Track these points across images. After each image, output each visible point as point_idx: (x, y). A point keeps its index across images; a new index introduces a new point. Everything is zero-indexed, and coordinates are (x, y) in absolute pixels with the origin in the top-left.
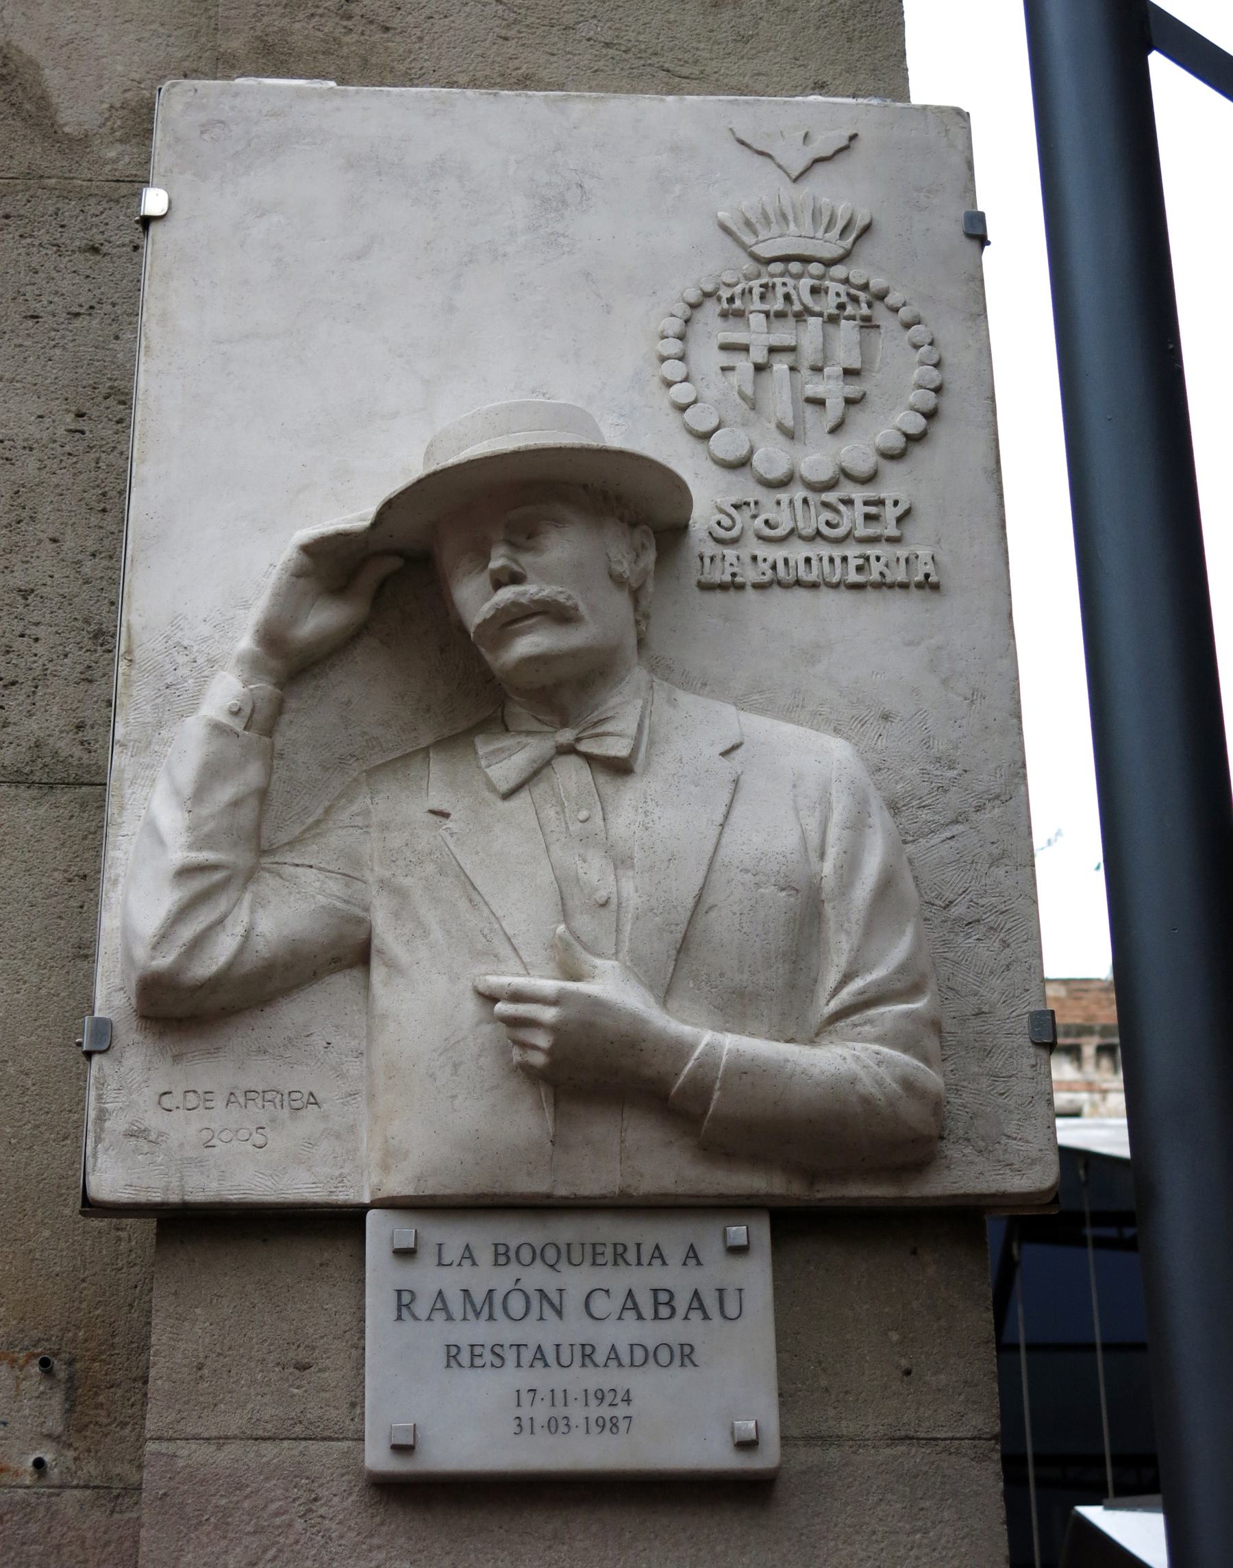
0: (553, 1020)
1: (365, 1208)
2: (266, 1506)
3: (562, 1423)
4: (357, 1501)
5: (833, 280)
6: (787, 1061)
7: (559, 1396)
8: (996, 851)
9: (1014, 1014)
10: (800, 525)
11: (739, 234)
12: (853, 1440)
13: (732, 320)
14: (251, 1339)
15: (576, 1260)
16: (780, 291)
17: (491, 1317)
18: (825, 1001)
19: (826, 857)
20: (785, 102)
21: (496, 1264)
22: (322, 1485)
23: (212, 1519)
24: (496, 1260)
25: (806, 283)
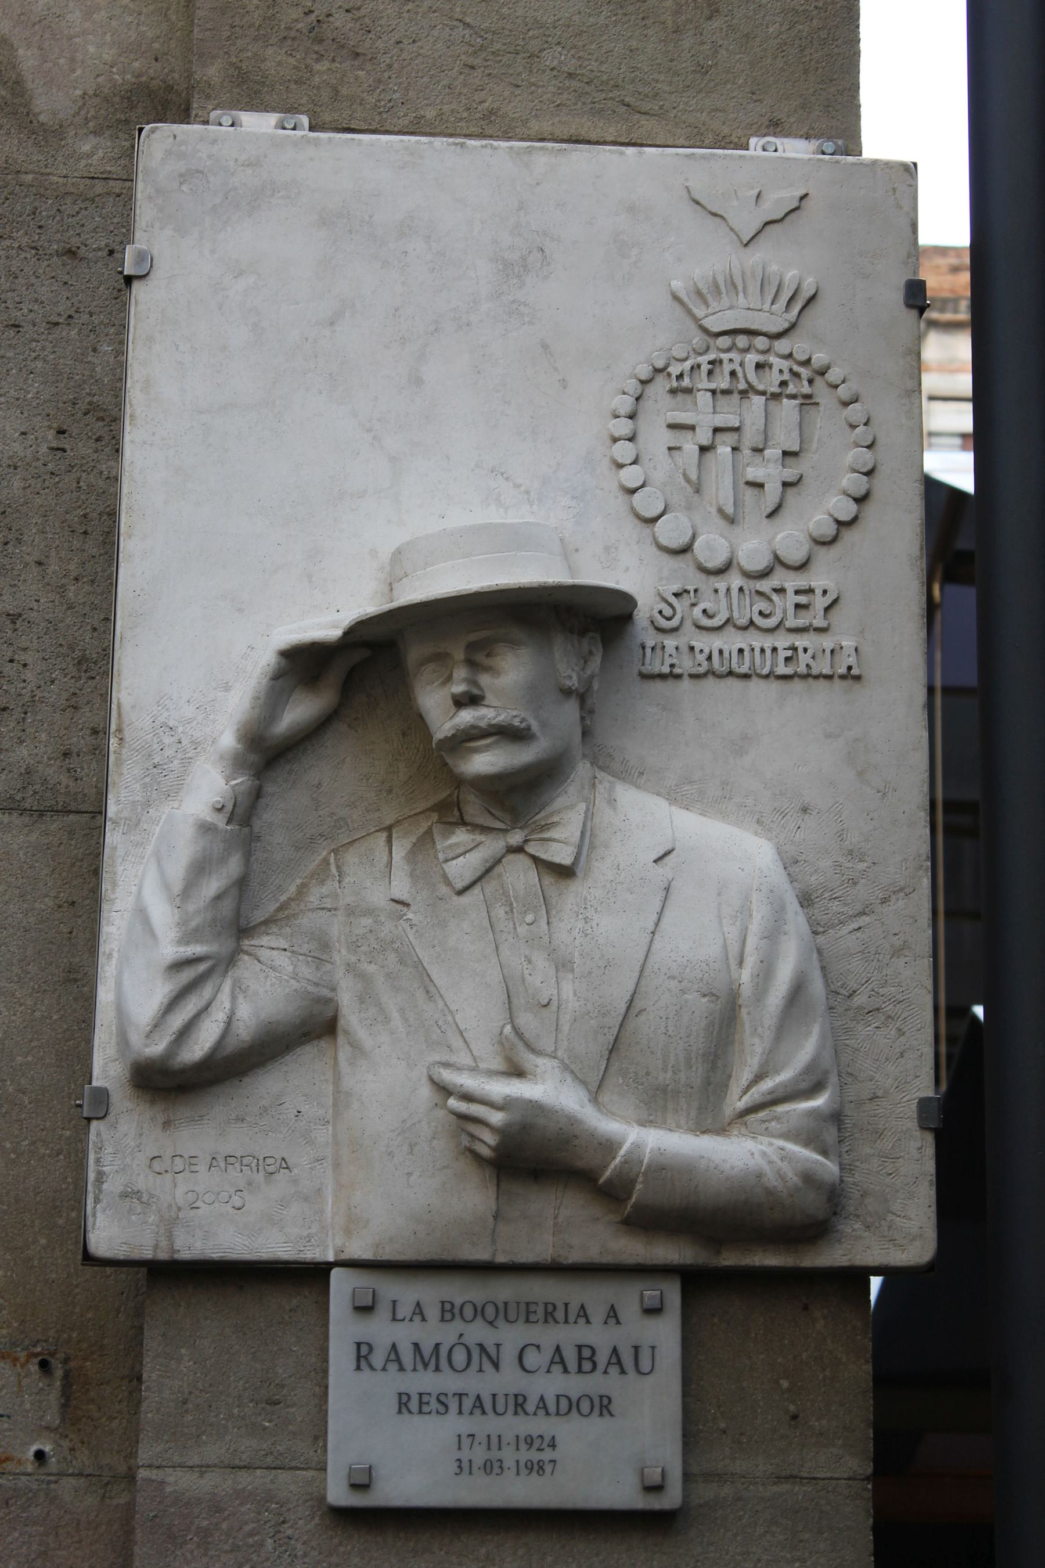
1: (330, 1266)
2: (241, 1528)
3: (496, 1465)
4: (319, 1525)
7: (494, 1440)
8: (897, 942)
9: (905, 1099)
10: (736, 615)
13: (680, 397)
16: (727, 368)
17: (437, 1369)
20: (741, 157)
21: (443, 1320)
22: (289, 1510)
23: (195, 1539)
24: (443, 1317)
25: (752, 358)
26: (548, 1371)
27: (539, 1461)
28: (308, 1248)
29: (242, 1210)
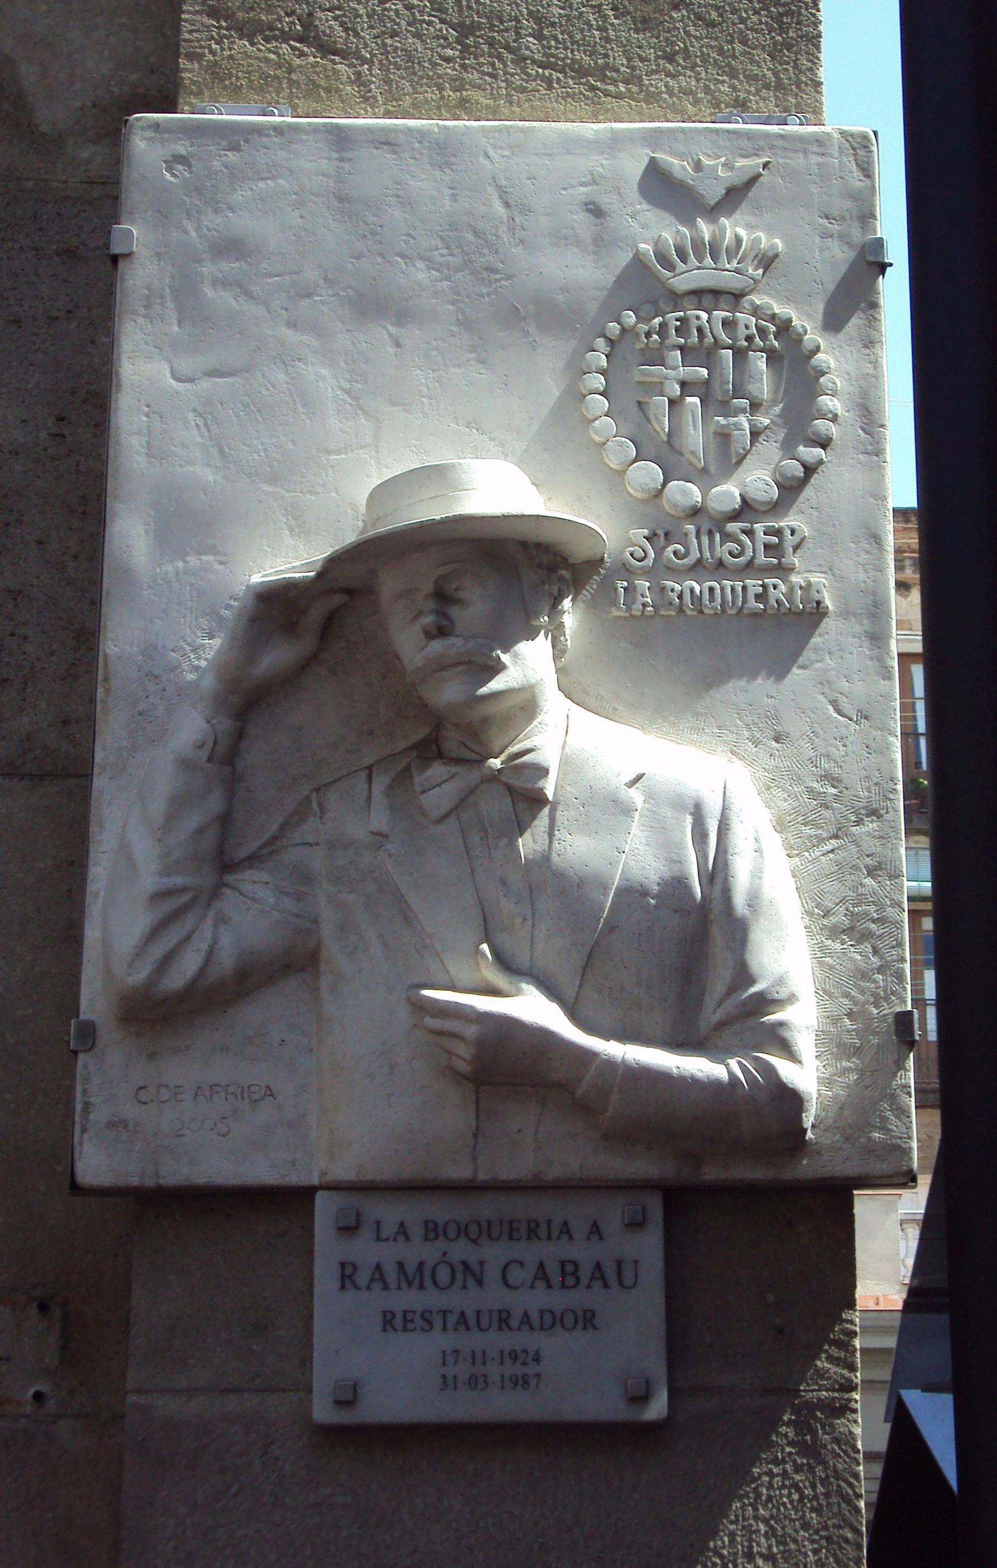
3: (481, 1380)
7: (479, 1356)
17: (421, 1286)
21: (426, 1239)
23: (183, 1461)
26: (532, 1287)
29: (227, 1137)
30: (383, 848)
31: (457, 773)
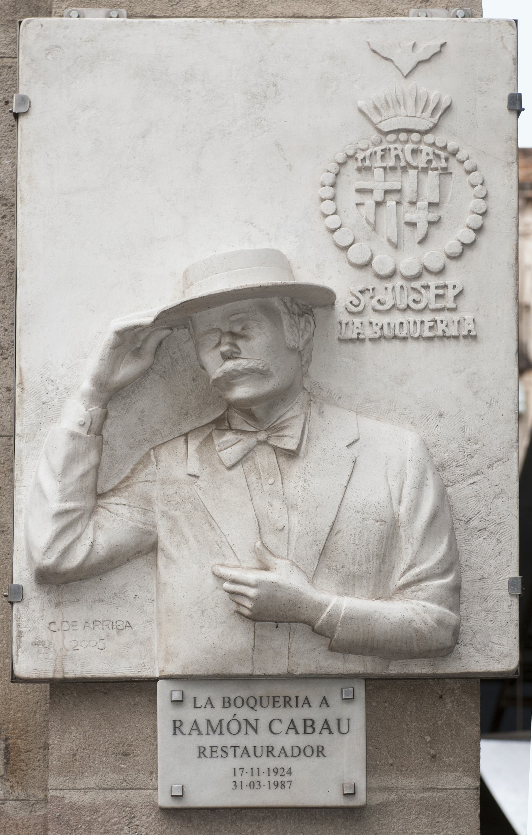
0: (254, 595)
2: (109, 821)
5: (426, 144)
6: (376, 612)
7: (255, 771)
8: (497, 489)
9: (501, 579)
10: (398, 302)
11: (370, 116)
12: (404, 789)
13: (364, 173)
14: (100, 741)
15: (264, 705)
16: (393, 153)
17: (221, 733)
18: (398, 578)
19: (402, 503)
20: (403, 21)
21: (224, 707)
22: (137, 811)
23: (83, 827)
25: (409, 147)
26: (287, 733)
27: (281, 782)
28: (144, 670)
29: (104, 650)
30: (196, 484)
31: (242, 439)
